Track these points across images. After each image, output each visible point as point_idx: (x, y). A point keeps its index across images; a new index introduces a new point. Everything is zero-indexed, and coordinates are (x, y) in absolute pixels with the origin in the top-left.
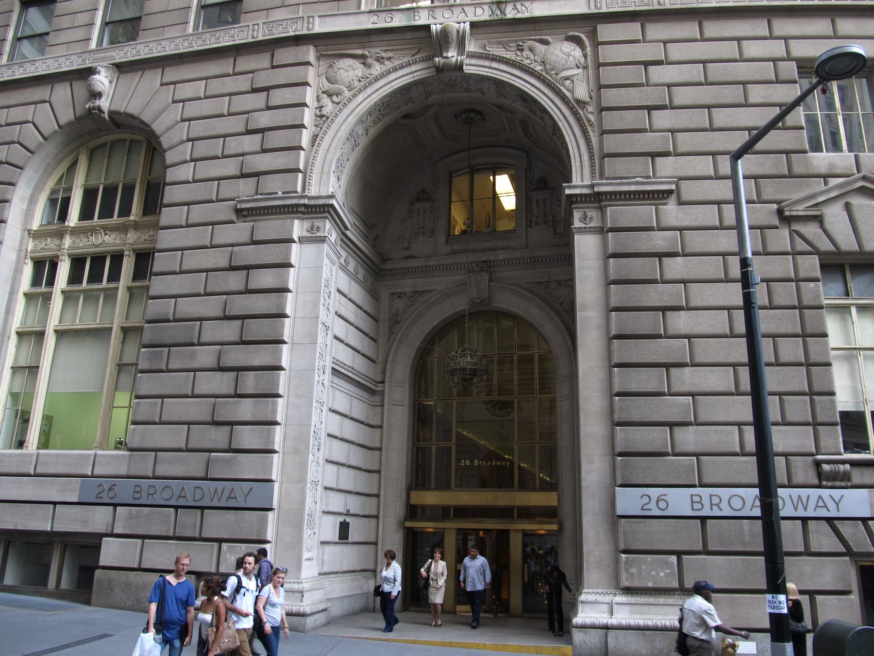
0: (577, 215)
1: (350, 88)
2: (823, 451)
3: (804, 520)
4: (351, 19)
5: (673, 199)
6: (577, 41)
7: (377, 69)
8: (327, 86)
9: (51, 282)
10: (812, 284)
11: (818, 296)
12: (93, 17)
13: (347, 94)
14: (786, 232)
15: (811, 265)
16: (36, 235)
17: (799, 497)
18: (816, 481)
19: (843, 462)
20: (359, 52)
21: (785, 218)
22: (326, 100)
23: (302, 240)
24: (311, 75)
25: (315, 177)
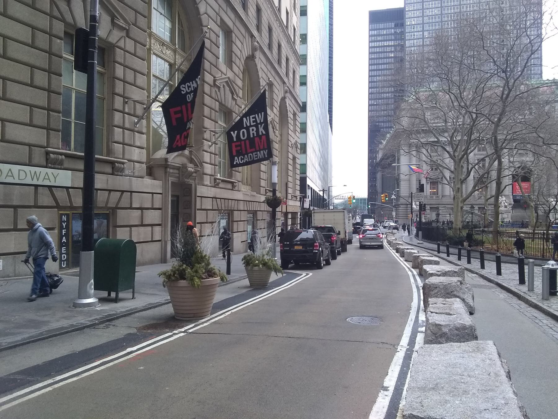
2: (51, 146)
3: (36, 186)
10: (59, 41)
15: (59, 28)
17: (35, 172)
18: (45, 164)
19: (61, 154)
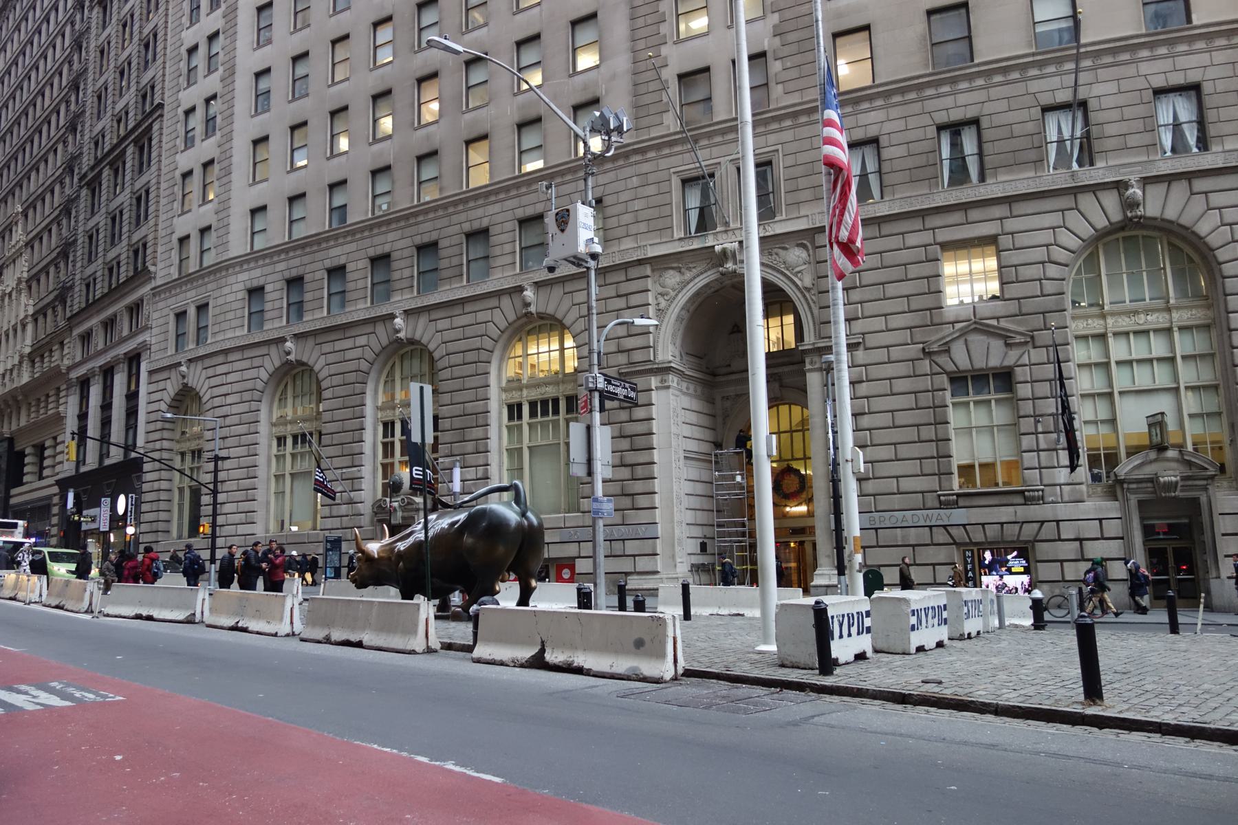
0: (807, 360)
1: (674, 290)
4: (669, 245)
5: (862, 347)
6: (804, 246)
7: (688, 275)
8: (660, 290)
9: (520, 417)
11: (944, 399)
12: (514, 247)
13: (673, 294)
14: (927, 362)
16: (504, 390)
20: (675, 265)
21: (927, 353)
22: (661, 299)
23: (657, 388)
24: (649, 283)
25: (660, 349)
